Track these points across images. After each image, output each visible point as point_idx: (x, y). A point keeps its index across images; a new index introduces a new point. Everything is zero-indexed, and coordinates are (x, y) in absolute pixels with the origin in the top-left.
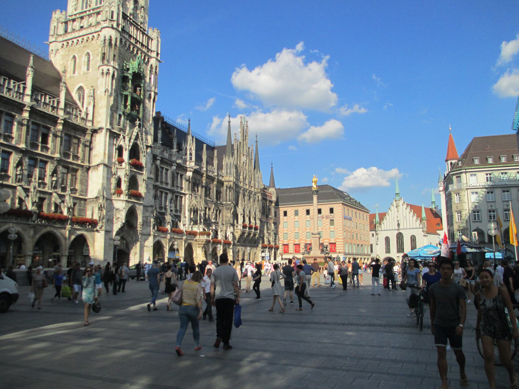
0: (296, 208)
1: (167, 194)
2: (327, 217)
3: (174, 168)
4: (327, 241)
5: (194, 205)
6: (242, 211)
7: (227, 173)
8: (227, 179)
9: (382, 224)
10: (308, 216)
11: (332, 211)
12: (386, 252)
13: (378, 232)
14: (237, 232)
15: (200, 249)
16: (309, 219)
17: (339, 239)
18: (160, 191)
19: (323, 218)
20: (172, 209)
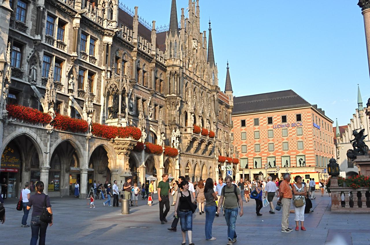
0: (256, 116)
1: (59, 62)
2: (293, 125)
3: (77, 22)
4: (295, 153)
5: (113, 86)
6: (193, 108)
7: (171, 56)
8: (171, 63)
9: (343, 136)
10: (270, 125)
11: (299, 117)
12: (349, 167)
13: (339, 145)
14: (186, 138)
15: (122, 156)
16: (272, 129)
17: (309, 150)
18: (45, 54)
19: (288, 127)
20: (71, 87)
